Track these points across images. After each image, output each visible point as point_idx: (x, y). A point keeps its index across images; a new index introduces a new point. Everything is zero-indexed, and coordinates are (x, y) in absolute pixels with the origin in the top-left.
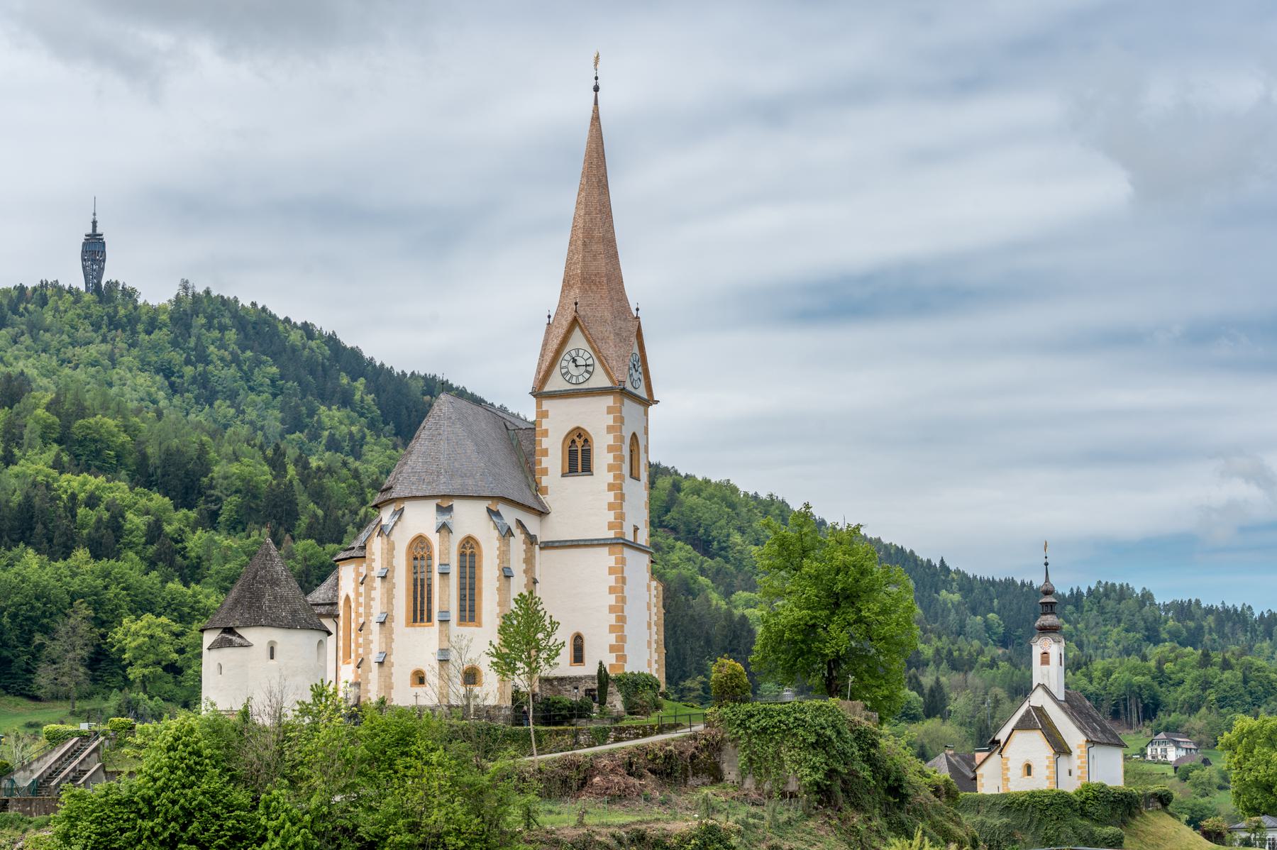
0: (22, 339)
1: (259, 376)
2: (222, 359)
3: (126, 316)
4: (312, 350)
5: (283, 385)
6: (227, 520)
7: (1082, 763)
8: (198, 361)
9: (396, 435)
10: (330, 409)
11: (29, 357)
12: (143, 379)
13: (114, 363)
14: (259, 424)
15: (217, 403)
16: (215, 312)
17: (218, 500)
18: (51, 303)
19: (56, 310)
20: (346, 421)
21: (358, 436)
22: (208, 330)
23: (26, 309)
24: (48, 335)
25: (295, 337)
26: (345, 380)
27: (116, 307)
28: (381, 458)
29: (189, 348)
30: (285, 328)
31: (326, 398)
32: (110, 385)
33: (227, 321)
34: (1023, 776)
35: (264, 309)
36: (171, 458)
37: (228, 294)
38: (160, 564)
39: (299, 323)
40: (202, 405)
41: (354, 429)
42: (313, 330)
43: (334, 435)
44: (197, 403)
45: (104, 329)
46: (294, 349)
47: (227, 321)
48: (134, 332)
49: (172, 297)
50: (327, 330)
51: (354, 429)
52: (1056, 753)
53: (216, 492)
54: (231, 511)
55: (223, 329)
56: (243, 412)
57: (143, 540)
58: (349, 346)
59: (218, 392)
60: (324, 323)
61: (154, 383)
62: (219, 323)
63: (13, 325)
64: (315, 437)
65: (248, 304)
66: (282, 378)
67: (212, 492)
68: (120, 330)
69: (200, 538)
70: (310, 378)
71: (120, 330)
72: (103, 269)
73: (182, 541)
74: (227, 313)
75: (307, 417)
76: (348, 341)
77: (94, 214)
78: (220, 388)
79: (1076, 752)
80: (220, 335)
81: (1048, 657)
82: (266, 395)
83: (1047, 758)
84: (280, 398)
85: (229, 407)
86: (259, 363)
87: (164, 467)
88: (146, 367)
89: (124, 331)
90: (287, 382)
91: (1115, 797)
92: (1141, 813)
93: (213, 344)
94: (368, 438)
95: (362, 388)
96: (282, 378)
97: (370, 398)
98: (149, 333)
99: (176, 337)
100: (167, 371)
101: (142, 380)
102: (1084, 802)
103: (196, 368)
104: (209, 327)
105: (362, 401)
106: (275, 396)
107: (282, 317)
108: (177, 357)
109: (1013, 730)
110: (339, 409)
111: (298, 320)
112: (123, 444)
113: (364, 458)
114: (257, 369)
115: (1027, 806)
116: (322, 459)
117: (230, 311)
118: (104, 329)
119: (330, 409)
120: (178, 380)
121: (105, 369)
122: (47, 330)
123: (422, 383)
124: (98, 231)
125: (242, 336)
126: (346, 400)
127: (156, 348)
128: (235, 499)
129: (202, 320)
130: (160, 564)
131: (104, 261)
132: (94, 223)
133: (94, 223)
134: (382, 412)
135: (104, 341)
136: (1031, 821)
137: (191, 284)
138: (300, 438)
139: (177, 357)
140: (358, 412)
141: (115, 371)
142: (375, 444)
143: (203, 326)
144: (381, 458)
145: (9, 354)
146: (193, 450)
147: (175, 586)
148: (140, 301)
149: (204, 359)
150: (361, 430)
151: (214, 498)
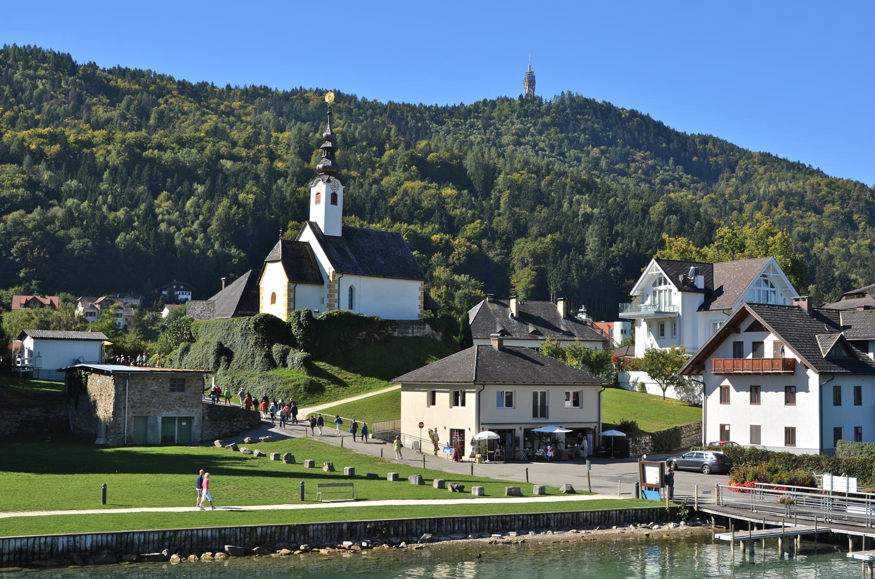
50: (645, 113)
60: (643, 110)
65: (600, 102)
124: (532, 70)
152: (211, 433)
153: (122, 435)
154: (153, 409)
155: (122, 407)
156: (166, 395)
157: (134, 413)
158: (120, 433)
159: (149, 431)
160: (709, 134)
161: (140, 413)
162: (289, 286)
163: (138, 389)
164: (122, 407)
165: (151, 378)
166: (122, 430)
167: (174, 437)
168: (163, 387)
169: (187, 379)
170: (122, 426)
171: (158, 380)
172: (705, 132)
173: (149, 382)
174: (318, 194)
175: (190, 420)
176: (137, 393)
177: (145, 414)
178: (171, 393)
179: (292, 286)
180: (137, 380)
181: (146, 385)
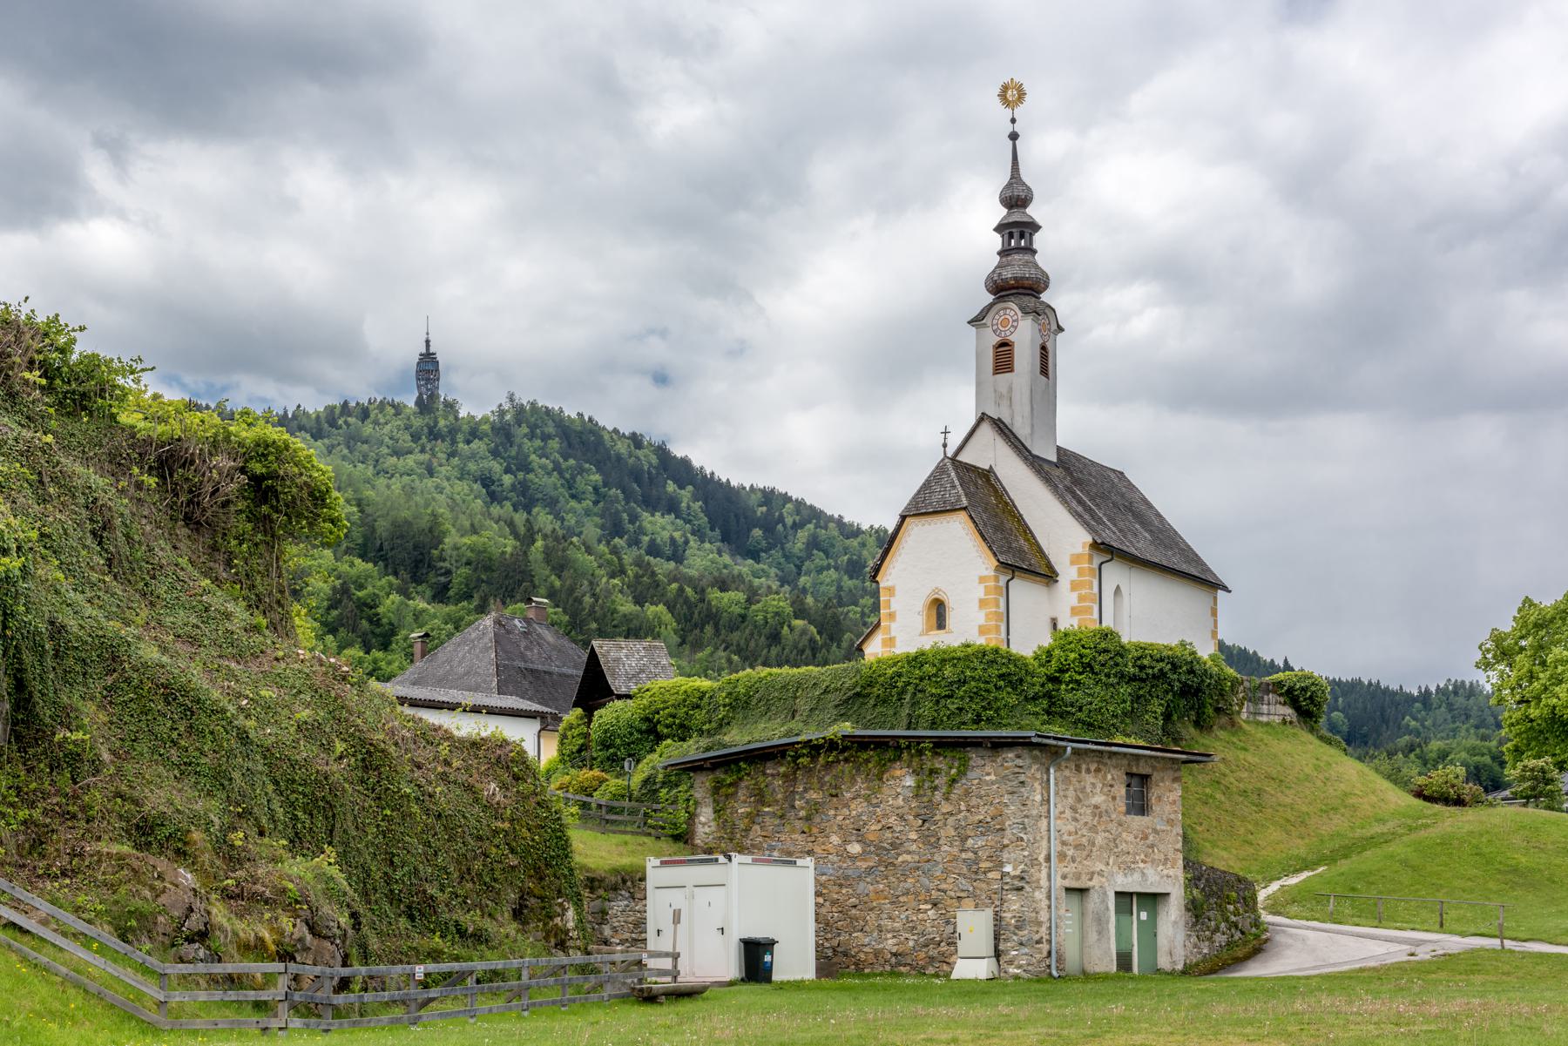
3: (446, 426)
4: (638, 458)
6: (456, 594)
7: (1081, 599)
8: (519, 470)
9: (723, 541)
10: (653, 515)
12: (462, 487)
15: (535, 510)
16: (539, 422)
17: (448, 572)
18: (372, 416)
19: (376, 423)
20: (669, 527)
21: (680, 541)
22: (530, 440)
23: (346, 422)
25: (622, 448)
26: (671, 487)
27: (436, 418)
29: (509, 457)
30: (611, 437)
31: (651, 504)
33: (551, 429)
34: (929, 629)
35: (590, 419)
36: (401, 530)
37: (553, 405)
38: (342, 629)
39: (627, 434)
41: (677, 535)
45: (424, 439)
46: (619, 457)
47: (551, 429)
48: (454, 442)
49: (495, 408)
52: (1004, 566)
53: (446, 564)
54: (461, 583)
55: (546, 438)
58: (679, 455)
59: (538, 500)
61: (472, 490)
62: (542, 433)
63: (328, 437)
65: (574, 416)
66: (605, 485)
67: (442, 564)
69: (393, 603)
70: (635, 486)
71: (439, 441)
73: (375, 606)
74: (550, 423)
76: (678, 451)
77: (428, 334)
78: (540, 496)
79: (1068, 574)
81: (1010, 354)
83: (982, 580)
84: (601, 504)
86: (582, 471)
87: (392, 539)
88: (466, 476)
89: (443, 441)
91: (1142, 668)
92: (1233, 724)
94: (692, 543)
95: (689, 495)
96: (605, 485)
98: (468, 442)
99: (497, 446)
100: (486, 481)
101: (460, 489)
102: (1053, 680)
103: (516, 477)
104: (532, 436)
105: (689, 507)
106: (596, 503)
107: (610, 428)
108: (496, 467)
109: (903, 518)
110: (663, 515)
111: (626, 430)
115: (903, 691)
117: (553, 421)
118: (424, 439)
119: (653, 515)
120: (499, 489)
122: (366, 442)
123: (759, 495)
125: (565, 444)
126: (672, 507)
127: (473, 456)
128: (464, 571)
129: (525, 430)
130: (342, 629)
131: (438, 380)
132: (428, 342)
133: (428, 342)
134: (710, 519)
135: (423, 451)
137: (517, 397)
139: (496, 467)
140: (684, 519)
142: (698, 549)
143: (526, 435)
146: (424, 523)
148: (463, 414)
149: (526, 467)
150: (684, 535)
151: (443, 571)
153: (1045, 947)
157: (1064, 877)
158: (1038, 942)
160: (771, 486)
161: (1078, 877)
164: (1041, 858)
168: (1114, 798)
169: (1155, 774)
171: (1105, 777)
172: (762, 483)
173: (1089, 779)
176: (1068, 813)
180: (1067, 773)
181: (1083, 790)
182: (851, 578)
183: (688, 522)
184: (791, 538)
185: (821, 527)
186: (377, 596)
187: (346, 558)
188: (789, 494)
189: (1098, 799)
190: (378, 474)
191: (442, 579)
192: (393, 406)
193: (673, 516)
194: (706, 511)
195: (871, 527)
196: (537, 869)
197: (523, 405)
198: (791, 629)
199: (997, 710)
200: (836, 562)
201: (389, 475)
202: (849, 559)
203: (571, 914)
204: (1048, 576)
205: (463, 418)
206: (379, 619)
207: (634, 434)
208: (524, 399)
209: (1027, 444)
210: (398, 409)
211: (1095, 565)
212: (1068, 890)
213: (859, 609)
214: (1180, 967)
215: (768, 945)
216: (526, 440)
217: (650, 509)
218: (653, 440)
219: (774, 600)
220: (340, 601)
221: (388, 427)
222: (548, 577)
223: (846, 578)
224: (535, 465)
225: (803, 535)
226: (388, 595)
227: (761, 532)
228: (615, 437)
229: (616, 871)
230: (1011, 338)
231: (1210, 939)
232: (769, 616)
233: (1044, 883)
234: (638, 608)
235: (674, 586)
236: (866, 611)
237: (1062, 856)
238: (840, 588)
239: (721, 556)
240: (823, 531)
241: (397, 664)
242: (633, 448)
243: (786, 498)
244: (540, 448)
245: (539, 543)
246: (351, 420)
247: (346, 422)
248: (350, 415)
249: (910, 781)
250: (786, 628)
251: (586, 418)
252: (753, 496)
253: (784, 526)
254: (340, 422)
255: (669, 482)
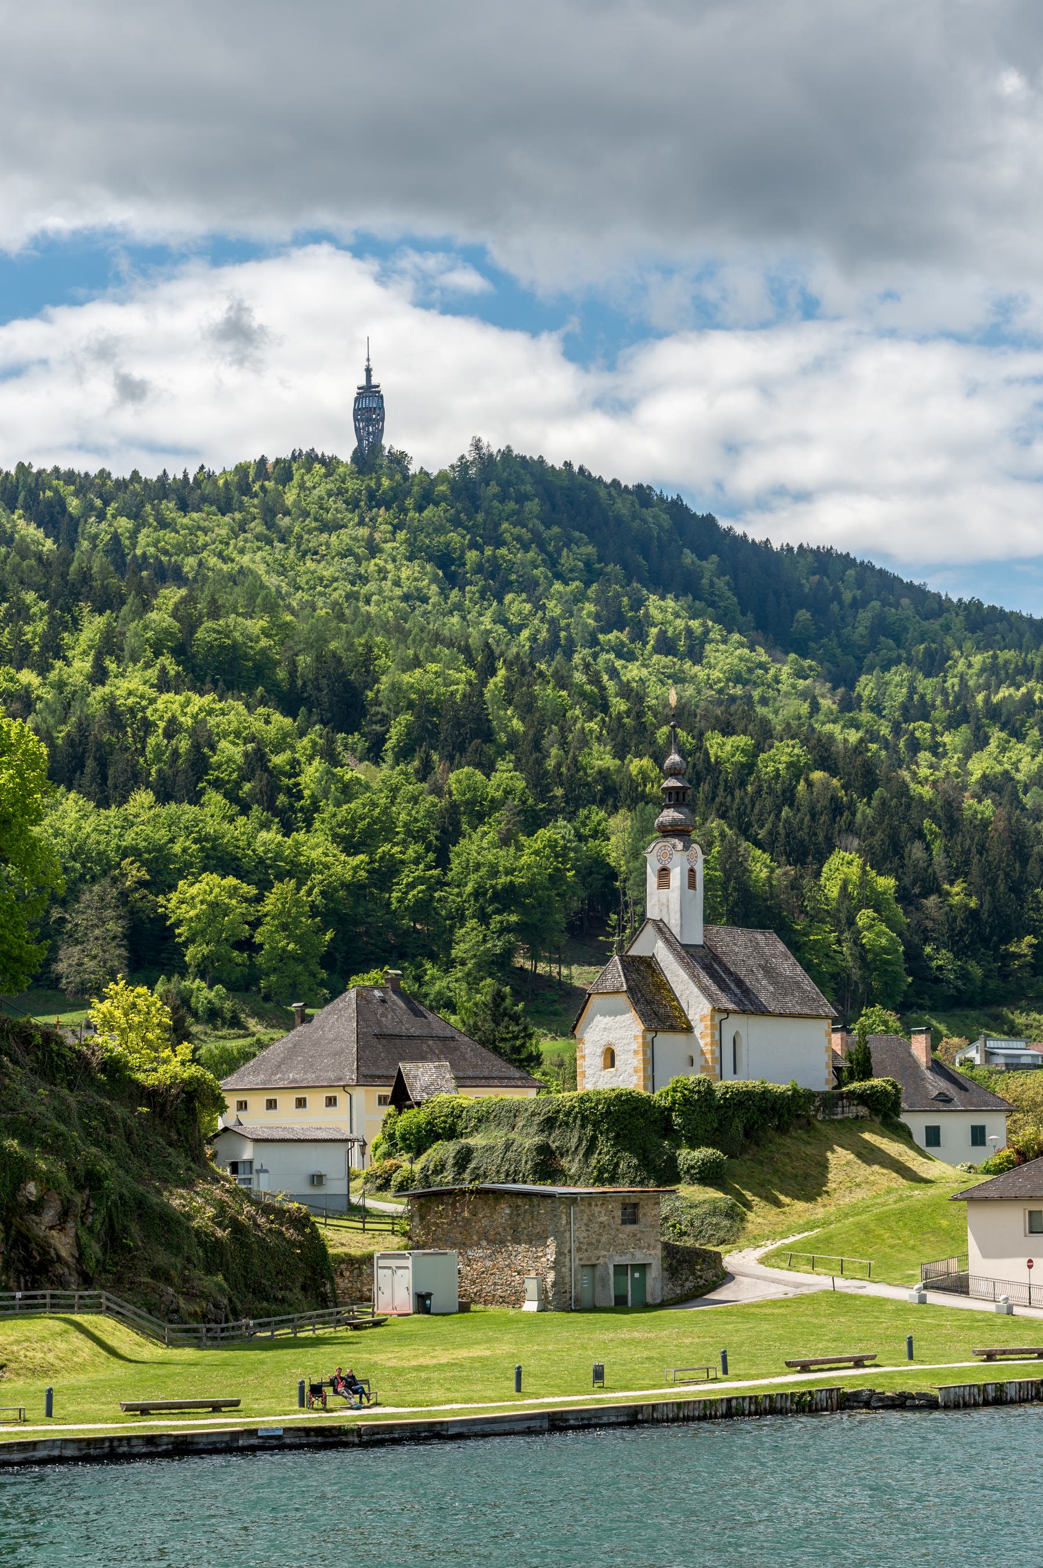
0: (253, 524)
1: (567, 560)
2: (518, 539)
5: (601, 568)
6: (394, 747)
9: (756, 629)
11: (259, 549)
13: (373, 550)
14: (563, 623)
15: (509, 597)
16: (513, 477)
18: (297, 477)
19: (302, 486)
20: (684, 613)
22: (501, 502)
23: (262, 487)
24: (287, 521)
26: (689, 557)
27: (378, 479)
28: (728, 661)
30: (609, 494)
31: (662, 585)
32: (364, 579)
34: (605, 1068)
35: (581, 469)
39: (630, 487)
40: (489, 600)
42: (650, 494)
43: (666, 632)
44: (483, 597)
46: (619, 520)
48: (404, 510)
49: (455, 461)
51: (695, 624)
52: (648, 1030)
53: (383, 709)
55: (522, 499)
56: (543, 607)
57: (235, 775)
58: (699, 513)
63: (241, 508)
64: (640, 635)
65: (559, 465)
67: (378, 709)
68: (383, 509)
71: (383, 509)
72: (382, 430)
74: (528, 478)
75: (631, 609)
77: (368, 360)
80: (517, 507)
82: (577, 583)
85: (524, 601)
89: (387, 509)
90: (606, 565)
91: (726, 1099)
92: (809, 1123)
93: (507, 520)
95: (713, 567)
97: (721, 583)
98: (420, 509)
99: (458, 512)
101: (409, 572)
105: (712, 584)
107: (608, 480)
112: (263, 651)
113: (705, 661)
114: (565, 550)
115: (575, 1118)
116: (646, 666)
117: (532, 475)
121: (359, 561)
122: (287, 513)
123: (810, 558)
124: (374, 382)
130: (255, 807)
131: (383, 420)
132: (368, 371)
133: (368, 371)
135: (361, 523)
136: (580, 1140)
137: (484, 443)
138: (618, 638)
140: (706, 600)
141: (373, 562)
143: (495, 496)
144: (728, 661)
145: (231, 547)
147: (270, 837)
148: (413, 469)
151: (379, 716)
152: (671, 1289)
153: (568, 1295)
154: (604, 1253)
155: (566, 1251)
156: (617, 1230)
157: (580, 1260)
158: (565, 1292)
159: (599, 1288)
161: (589, 1259)
162: (644, 1037)
163: (585, 1221)
164: (566, 1251)
165: (599, 1203)
166: (567, 1287)
167: (626, 1297)
168: (613, 1217)
169: (641, 1202)
170: (567, 1280)
173: (598, 1209)
174: (664, 869)
175: (643, 1268)
176: (583, 1228)
177: (594, 1261)
178: (623, 1227)
179: (650, 1036)
181: (593, 1215)
182: (928, 675)
183: (712, 604)
184: (849, 619)
185: (890, 605)
186: (299, 763)
187: (261, 710)
188: (852, 556)
189: (603, 1219)
190: (304, 555)
191: (377, 728)
192: (323, 461)
193: (691, 597)
194: (735, 590)
195: (960, 600)
196: (312, 1267)
197: (491, 455)
198: (810, 784)
199: (630, 1131)
200: (909, 653)
201: (318, 557)
202: (926, 648)
203: (328, 1286)
204: (689, 1029)
205: (415, 475)
206: (300, 791)
207: (640, 487)
208: (494, 444)
209: (678, 938)
210: (330, 464)
211: (717, 1021)
212: (583, 1266)
213: (928, 725)
214: (658, 1301)
215: (429, 1296)
216: (495, 503)
217: (661, 590)
218: (665, 494)
219: (788, 746)
220: (253, 771)
221: (316, 492)
222: (510, 720)
223: (920, 676)
224: (507, 536)
225: (865, 617)
226: (310, 759)
227: (808, 615)
228: (613, 492)
229: (363, 1256)
230: (669, 866)
231: (682, 1286)
232: (781, 766)
233: (567, 1263)
234: (618, 762)
235: (665, 729)
236: (939, 728)
237: (579, 1249)
238: (912, 690)
239: (753, 650)
240: (893, 610)
241: (321, 850)
242: (637, 506)
243: (846, 560)
244: (514, 513)
245: (502, 673)
246: (269, 485)
247: (262, 487)
248: (268, 479)
249: (508, 1211)
250: (802, 782)
251: (576, 469)
252: (802, 561)
253: (841, 604)
254: (256, 487)
255: (687, 551)
